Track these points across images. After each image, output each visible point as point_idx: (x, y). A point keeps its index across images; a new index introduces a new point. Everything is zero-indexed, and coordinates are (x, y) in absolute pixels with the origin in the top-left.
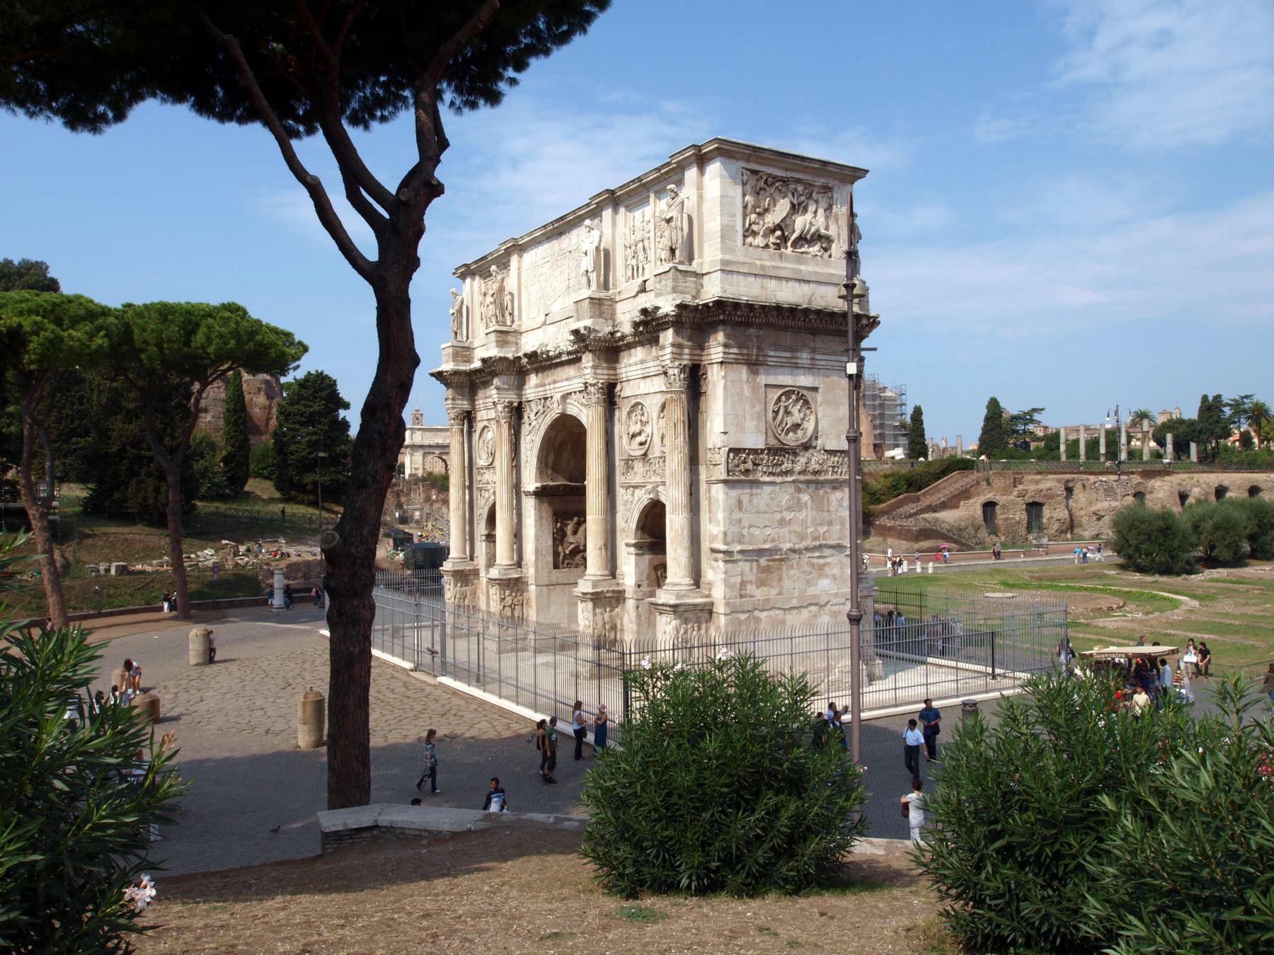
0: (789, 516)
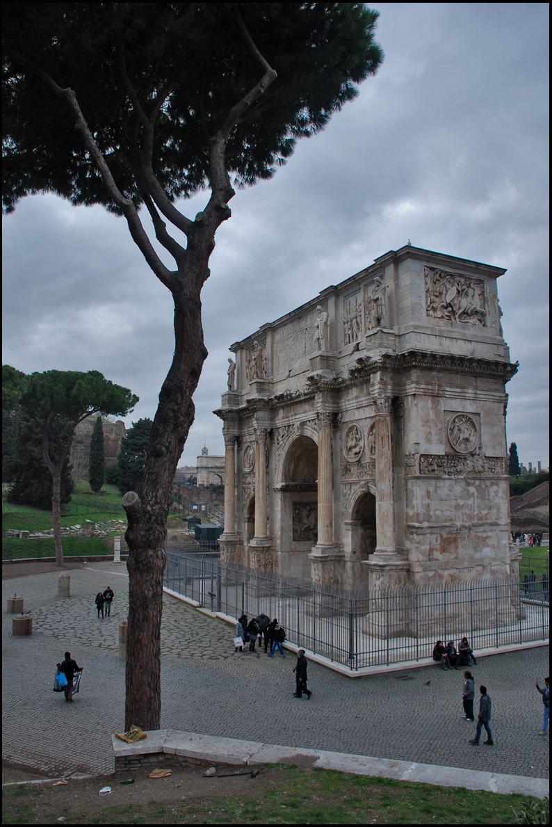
0: (461, 502)
